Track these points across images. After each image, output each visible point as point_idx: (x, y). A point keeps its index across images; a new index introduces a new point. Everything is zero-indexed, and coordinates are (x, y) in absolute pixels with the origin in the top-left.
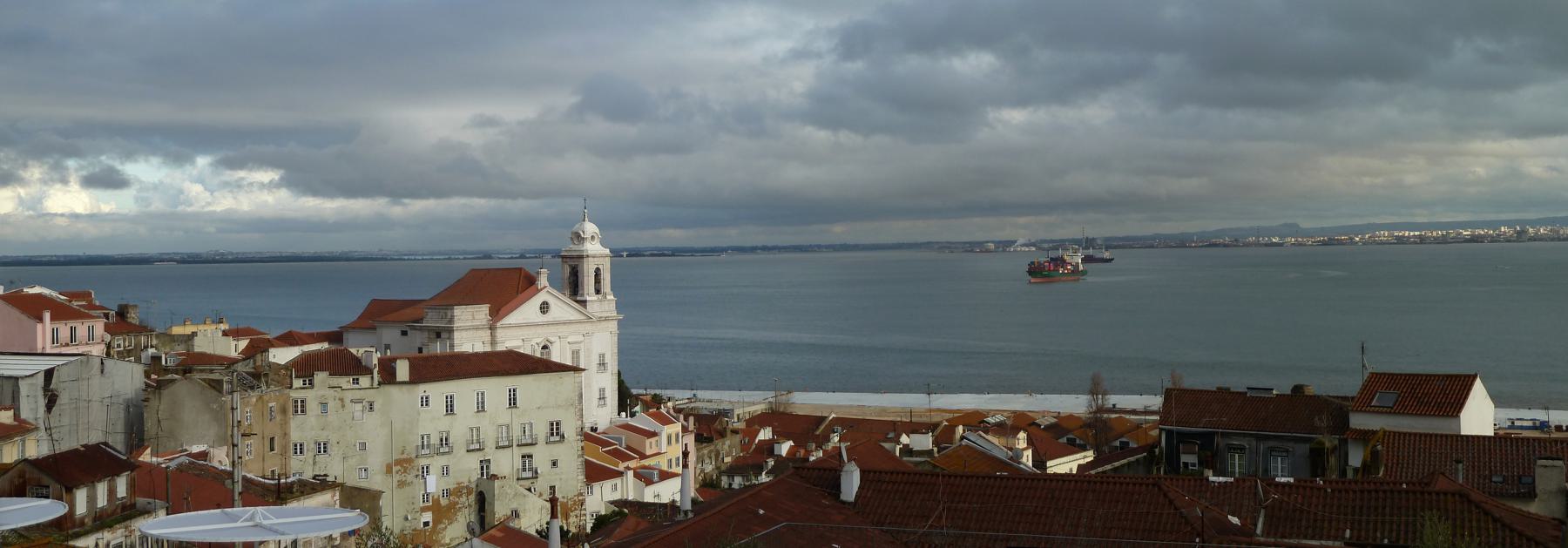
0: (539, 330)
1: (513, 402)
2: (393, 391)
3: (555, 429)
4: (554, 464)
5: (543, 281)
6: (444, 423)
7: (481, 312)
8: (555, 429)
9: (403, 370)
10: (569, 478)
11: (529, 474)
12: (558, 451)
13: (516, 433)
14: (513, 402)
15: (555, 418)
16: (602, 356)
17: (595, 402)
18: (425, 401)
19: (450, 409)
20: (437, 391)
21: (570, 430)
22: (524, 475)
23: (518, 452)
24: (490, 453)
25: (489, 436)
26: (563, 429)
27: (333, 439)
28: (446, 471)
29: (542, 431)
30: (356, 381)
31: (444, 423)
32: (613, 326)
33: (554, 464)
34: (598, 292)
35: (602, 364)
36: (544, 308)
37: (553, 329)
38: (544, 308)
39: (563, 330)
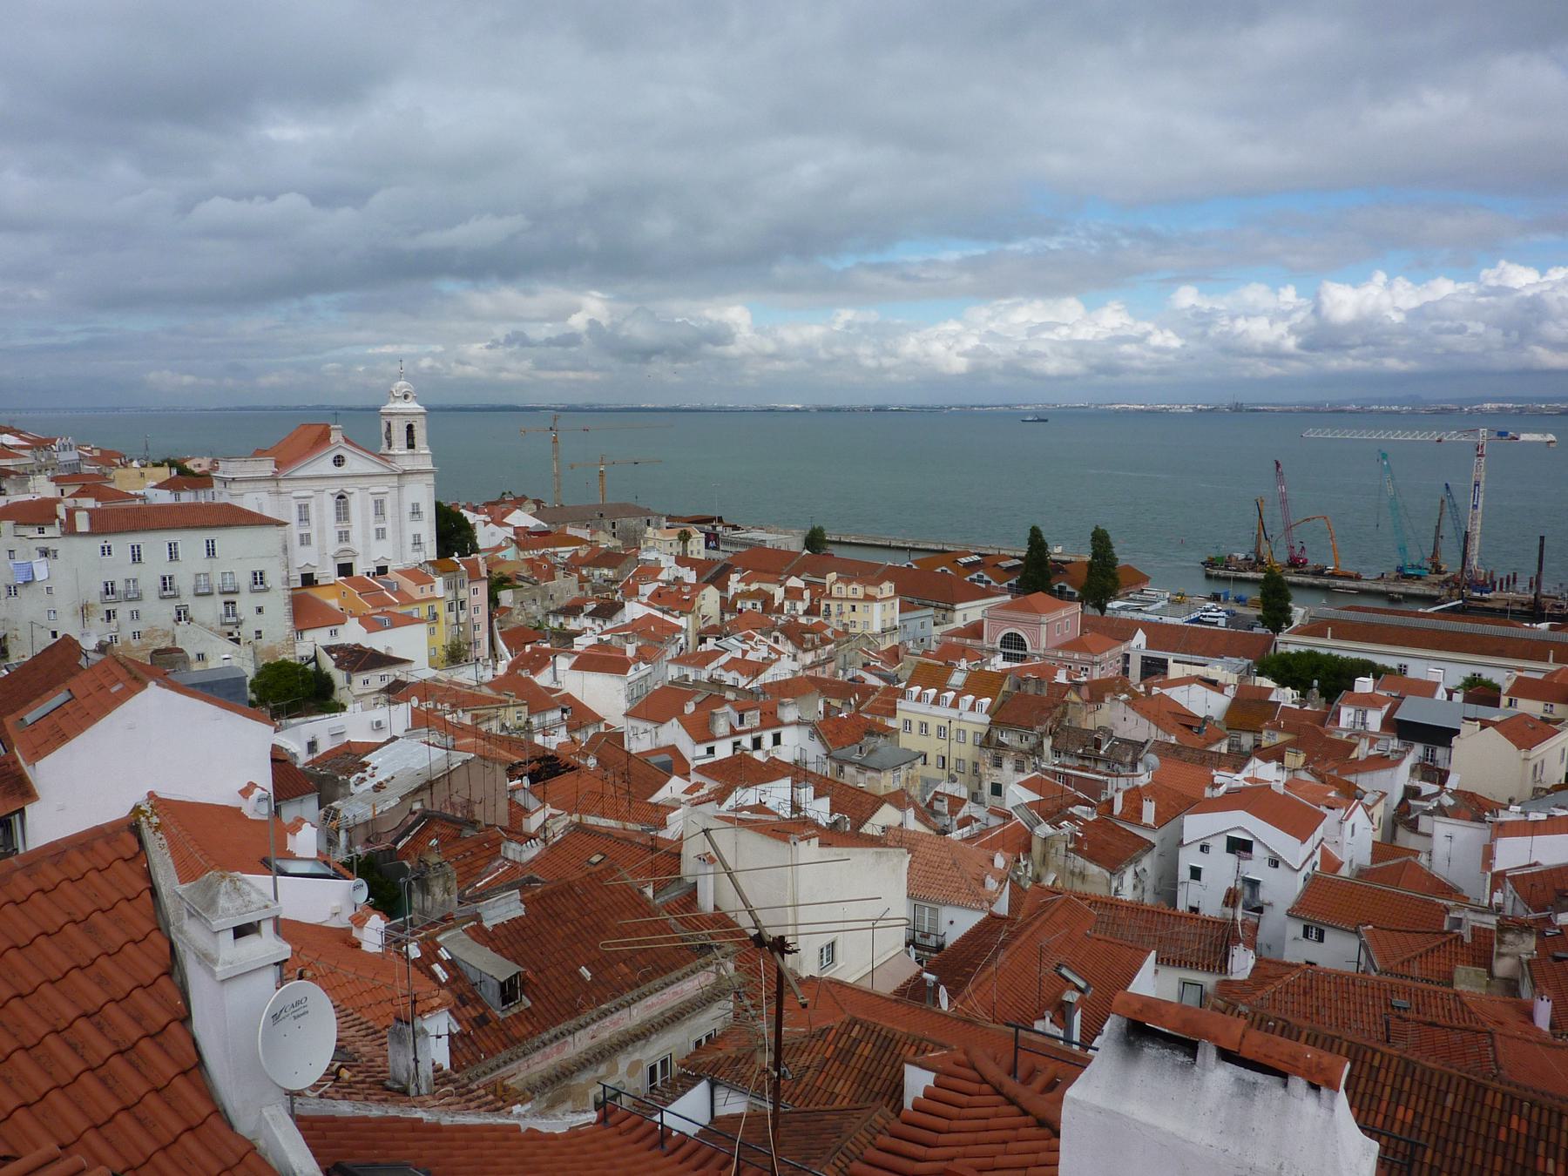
0: (338, 482)
1: (211, 552)
2: (76, 542)
3: (258, 578)
4: (260, 610)
5: (336, 437)
7: (267, 467)
8: (258, 578)
9: (82, 524)
11: (234, 620)
12: (261, 600)
13: (217, 581)
14: (211, 552)
15: (258, 568)
18: (106, 551)
19: (136, 557)
20: (121, 544)
21: (274, 578)
22: (229, 620)
23: (221, 600)
25: (184, 583)
26: (267, 577)
28: (135, 615)
29: (244, 580)
30: (41, 531)
31: (133, 571)
32: (430, 479)
33: (260, 610)
34: (411, 446)
35: (416, 512)
36: (339, 461)
37: (351, 481)
38: (339, 461)
39: (364, 482)
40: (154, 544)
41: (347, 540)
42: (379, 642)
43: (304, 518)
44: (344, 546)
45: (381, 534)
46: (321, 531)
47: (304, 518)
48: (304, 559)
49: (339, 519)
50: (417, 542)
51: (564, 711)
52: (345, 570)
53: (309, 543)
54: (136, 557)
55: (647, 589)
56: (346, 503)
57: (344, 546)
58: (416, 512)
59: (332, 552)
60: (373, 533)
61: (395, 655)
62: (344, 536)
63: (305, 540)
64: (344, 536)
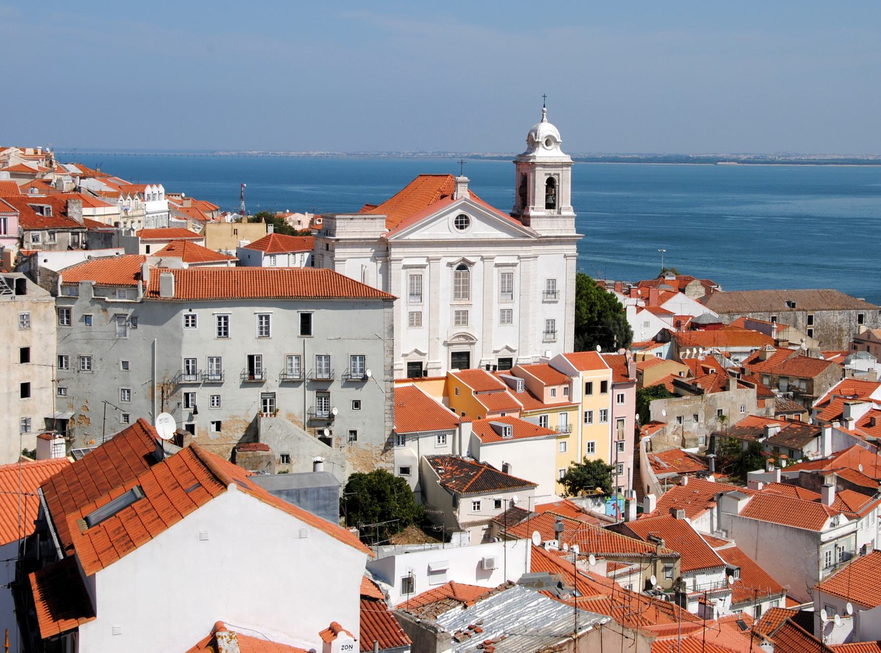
4: (357, 404)
6: (217, 347)
10: (373, 421)
16: (552, 282)
17: (540, 336)
18: (192, 321)
19: (223, 331)
24: (272, 384)
27: (96, 355)
28: (216, 401)
29: (340, 367)
31: (217, 347)
32: (572, 249)
33: (357, 404)
34: (550, 206)
36: (462, 222)
38: (462, 222)
40: (244, 318)
41: (465, 322)
42: (493, 456)
43: (416, 294)
44: (462, 329)
45: (506, 316)
46: (434, 310)
47: (416, 294)
48: (409, 343)
49: (457, 295)
50: (550, 330)
51: (730, 572)
52: (461, 360)
53: (419, 324)
54: (223, 331)
55: (858, 412)
56: (467, 275)
57: (462, 329)
58: (551, 291)
59: (444, 337)
60: (496, 316)
61: (513, 473)
62: (462, 317)
63: (415, 319)
64: (462, 317)
